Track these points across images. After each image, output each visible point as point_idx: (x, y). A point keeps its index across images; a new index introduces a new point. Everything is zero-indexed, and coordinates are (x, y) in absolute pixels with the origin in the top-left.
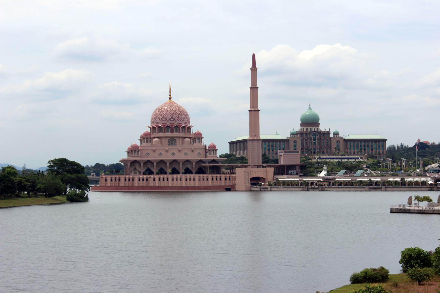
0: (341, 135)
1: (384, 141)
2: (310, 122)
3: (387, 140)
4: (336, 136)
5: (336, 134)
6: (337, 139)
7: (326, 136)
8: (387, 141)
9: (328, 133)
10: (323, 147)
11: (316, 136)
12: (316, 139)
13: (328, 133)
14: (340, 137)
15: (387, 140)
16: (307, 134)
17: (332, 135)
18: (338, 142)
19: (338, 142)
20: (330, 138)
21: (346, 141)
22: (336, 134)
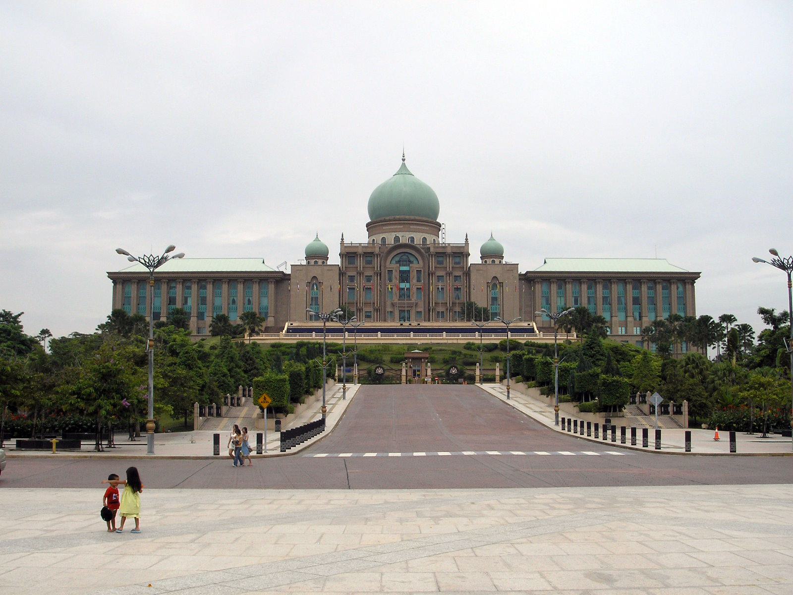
0: (507, 259)
1: (688, 280)
2: (403, 215)
3: (697, 275)
4: (489, 261)
5: (492, 254)
6: (494, 271)
7: (449, 263)
8: (698, 284)
9: (461, 253)
10: (441, 309)
11: (411, 262)
12: (414, 274)
13: (461, 253)
14: (506, 264)
15: (697, 275)
16: (372, 254)
17: (475, 258)
18: (495, 283)
19: (495, 283)
20: (468, 273)
21: (530, 279)
22: (492, 254)
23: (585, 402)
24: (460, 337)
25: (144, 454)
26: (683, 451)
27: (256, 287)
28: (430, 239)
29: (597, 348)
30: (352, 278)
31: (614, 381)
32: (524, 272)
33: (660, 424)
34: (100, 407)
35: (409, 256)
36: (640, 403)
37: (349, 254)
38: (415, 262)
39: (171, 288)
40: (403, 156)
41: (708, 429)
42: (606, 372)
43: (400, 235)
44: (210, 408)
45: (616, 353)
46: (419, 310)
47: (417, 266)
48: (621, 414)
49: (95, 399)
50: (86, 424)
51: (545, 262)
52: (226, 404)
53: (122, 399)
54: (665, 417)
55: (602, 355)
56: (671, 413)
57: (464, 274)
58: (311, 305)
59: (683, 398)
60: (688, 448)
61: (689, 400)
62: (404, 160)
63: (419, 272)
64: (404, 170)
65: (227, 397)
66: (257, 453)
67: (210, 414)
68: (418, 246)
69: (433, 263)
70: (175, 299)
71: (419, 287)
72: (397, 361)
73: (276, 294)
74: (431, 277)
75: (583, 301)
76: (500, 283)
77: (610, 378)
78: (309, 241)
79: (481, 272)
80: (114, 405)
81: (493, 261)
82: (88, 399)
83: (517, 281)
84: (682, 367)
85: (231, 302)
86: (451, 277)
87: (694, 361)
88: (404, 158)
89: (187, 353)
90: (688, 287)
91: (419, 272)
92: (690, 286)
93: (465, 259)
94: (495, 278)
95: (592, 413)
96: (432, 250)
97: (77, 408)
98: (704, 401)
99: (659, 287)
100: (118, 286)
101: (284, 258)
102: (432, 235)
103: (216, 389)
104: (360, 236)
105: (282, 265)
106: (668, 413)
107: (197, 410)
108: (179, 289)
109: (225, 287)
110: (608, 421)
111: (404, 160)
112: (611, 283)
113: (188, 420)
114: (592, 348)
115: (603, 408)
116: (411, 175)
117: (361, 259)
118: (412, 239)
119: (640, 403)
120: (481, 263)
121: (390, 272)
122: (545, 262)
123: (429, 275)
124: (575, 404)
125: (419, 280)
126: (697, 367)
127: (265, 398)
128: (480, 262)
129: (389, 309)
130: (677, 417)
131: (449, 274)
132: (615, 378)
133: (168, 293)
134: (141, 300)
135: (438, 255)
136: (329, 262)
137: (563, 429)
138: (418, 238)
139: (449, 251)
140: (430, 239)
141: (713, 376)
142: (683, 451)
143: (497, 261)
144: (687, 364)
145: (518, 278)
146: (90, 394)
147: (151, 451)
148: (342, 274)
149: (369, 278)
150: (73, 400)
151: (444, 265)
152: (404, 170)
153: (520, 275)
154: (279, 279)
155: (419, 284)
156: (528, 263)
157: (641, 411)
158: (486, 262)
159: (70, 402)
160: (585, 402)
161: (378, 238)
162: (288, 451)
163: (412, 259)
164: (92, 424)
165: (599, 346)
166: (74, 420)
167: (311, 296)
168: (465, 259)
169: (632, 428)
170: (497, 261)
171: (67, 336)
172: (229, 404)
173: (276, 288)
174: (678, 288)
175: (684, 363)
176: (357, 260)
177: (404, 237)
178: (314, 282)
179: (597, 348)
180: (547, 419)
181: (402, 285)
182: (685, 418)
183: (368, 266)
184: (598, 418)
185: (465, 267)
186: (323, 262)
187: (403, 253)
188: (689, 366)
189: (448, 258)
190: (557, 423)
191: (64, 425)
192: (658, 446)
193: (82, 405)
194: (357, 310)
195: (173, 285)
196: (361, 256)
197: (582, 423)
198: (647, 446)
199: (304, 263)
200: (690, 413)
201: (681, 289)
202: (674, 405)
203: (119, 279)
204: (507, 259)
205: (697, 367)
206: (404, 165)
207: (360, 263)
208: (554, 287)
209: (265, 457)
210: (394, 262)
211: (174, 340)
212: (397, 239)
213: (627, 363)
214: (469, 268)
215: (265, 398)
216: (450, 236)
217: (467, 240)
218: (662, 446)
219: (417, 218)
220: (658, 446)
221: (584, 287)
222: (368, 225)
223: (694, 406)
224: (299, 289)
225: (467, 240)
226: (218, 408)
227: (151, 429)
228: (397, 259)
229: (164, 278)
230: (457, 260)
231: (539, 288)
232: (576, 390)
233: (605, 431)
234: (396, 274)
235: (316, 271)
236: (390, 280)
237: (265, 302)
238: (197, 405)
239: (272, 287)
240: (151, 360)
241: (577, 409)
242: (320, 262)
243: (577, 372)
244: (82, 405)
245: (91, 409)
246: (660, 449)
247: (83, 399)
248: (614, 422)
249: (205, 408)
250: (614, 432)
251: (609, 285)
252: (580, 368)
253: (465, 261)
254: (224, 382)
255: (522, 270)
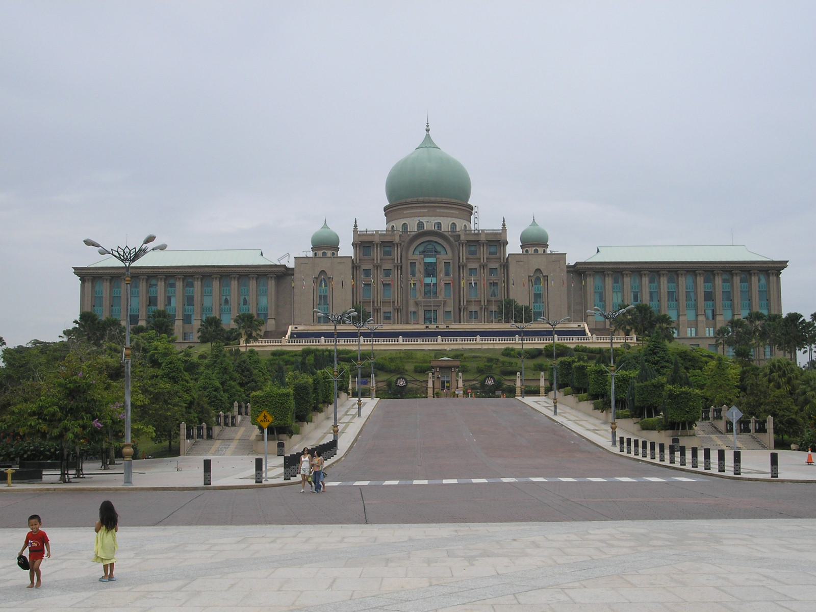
0: (553, 247)
1: (771, 270)
2: (428, 197)
3: (783, 265)
4: (531, 250)
5: (534, 242)
6: (537, 262)
7: (483, 253)
8: (784, 275)
9: (497, 241)
10: (473, 308)
12: (441, 267)
13: (497, 241)
14: (551, 254)
15: (783, 265)
17: (514, 247)
19: (538, 277)
21: (580, 271)
22: (534, 242)
23: (647, 417)
24: (497, 342)
25: (120, 485)
26: (769, 476)
27: (253, 284)
28: (460, 224)
29: (661, 354)
30: (367, 273)
31: (683, 393)
32: (572, 263)
33: (739, 444)
34: (66, 429)
35: (434, 244)
36: (714, 418)
37: (364, 243)
38: (443, 252)
39: (151, 286)
40: (428, 126)
41: (799, 450)
42: (673, 381)
43: (424, 220)
44: (200, 429)
45: (684, 359)
46: (448, 309)
47: (445, 257)
48: (692, 432)
49: (60, 420)
50: (49, 450)
51: (598, 251)
52: (219, 424)
53: (94, 419)
54: (745, 436)
55: (667, 361)
56: (753, 431)
57: (501, 266)
58: (318, 305)
59: (767, 412)
60: (775, 473)
61: (774, 415)
62: (428, 130)
63: (447, 264)
64: (428, 142)
65: (220, 416)
66: (256, 482)
67: (200, 436)
68: (446, 233)
69: (464, 252)
70: (156, 298)
71: (448, 282)
72: (422, 371)
73: (277, 292)
74: (461, 270)
75: (644, 298)
76: (544, 276)
77: (677, 390)
78: (315, 228)
79: (521, 263)
80: (84, 427)
81: (536, 251)
82: (52, 420)
83: (564, 274)
84: (765, 375)
85: (223, 301)
86: (485, 270)
87: (780, 368)
88: (428, 128)
89: (171, 363)
90: (773, 279)
91: (447, 264)
92: (775, 278)
93: (502, 248)
94: (538, 270)
95: (657, 432)
96: (462, 238)
97: (39, 431)
98: (794, 417)
99: (737, 280)
100: (86, 284)
101: (286, 248)
102: (462, 220)
103: (206, 406)
104: (376, 222)
105: (282, 258)
106: (749, 431)
107: (183, 432)
108: (160, 288)
109: (216, 284)
110: (676, 441)
111: (428, 130)
112: (678, 275)
113: (172, 443)
114: (655, 353)
115: (671, 426)
116: (437, 148)
117: (379, 249)
118: (439, 225)
119: (714, 418)
120: (521, 253)
121: (413, 264)
122: (598, 251)
123: (459, 267)
124: (635, 420)
125: (447, 274)
126: (784, 375)
127: (265, 416)
128: (520, 251)
129: (412, 308)
130: (760, 436)
131: (483, 266)
132: (683, 389)
133: (147, 292)
134: (114, 300)
135: (469, 243)
136: (340, 254)
137: (622, 450)
138: (446, 224)
139: (483, 238)
140: (460, 224)
141: (804, 387)
142: (769, 476)
143: (540, 250)
144: (772, 372)
145: (565, 270)
146: (54, 414)
147: (128, 481)
148: (355, 267)
149: (387, 273)
150: (33, 421)
151: (478, 256)
152: (428, 142)
153: (568, 266)
154: (281, 274)
155: (447, 278)
156: (577, 254)
157: (716, 428)
158: (527, 251)
159: (29, 424)
160: (647, 417)
161: (398, 224)
162: (293, 479)
163: (439, 248)
164: (56, 450)
165: (665, 351)
166: (33, 445)
167: (319, 294)
168: (502, 248)
169: (705, 450)
170: (540, 250)
171: (25, 346)
172: (222, 424)
173: (278, 285)
174: (759, 281)
175: (768, 371)
176: (374, 251)
177: (430, 223)
178: (323, 278)
179: (661, 354)
180: (603, 440)
181: (428, 280)
182: (770, 437)
183: (387, 257)
184: (663, 437)
185: (502, 258)
186: (333, 254)
187: (427, 241)
188: (774, 374)
189: (482, 248)
190: (614, 443)
191: (22, 452)
192: (737, 471)
193: (44, 427)
194: (374, 310)
195: (153, 282)
196: (379, 246)
197: (644, 443)
198: (724, 471)
199: (311, 254)
200: (777, 431)
201: (763, 281)
202: (756, 422)
203: (87, 276)
204: (553, 247)
205: (784, 375)
206: (428, 137)
207: (377, 254)
208: (609, 281)
209: (265, 486)
210: (417, 252)
211: (156, 349)
212: (421, 225)
213: (697, 371)
214: (507, 259)
215: (265, 416)
216: (484, 220)
217: (504, 225)
218: (742, 470)
219: (444, 199)
220: (737, 471)
221: (645, 280)
222: (385, 209)
223: (781, 422)
224: (304, 286)
225: (504, 225)
226: (209, 429)
227: (128, 455)
228: (421, 249)
229: (143, 274)
230: (493, 249)
231: (591, 283)
232: (637, 404)
233: (672, 452)
234: (419, 268)
235: (324, 265)
236: (413, 275)
237: (264, 301)
238: (183, 425)
239: (272, 284)
240: (128, 372)
241: (638, 426)
242: (329, 253)
243: (638, 383)
244: (44, 427)
245: (56, 432)
246: (740, 474)
247: (45, 420)
248: (683, 442)
249: (193, 429)
250: (683, 454)
251: (675, 277)
252: (642, 377)
253: (502, 251)
254: (216, 397)
255: (571, 261)
